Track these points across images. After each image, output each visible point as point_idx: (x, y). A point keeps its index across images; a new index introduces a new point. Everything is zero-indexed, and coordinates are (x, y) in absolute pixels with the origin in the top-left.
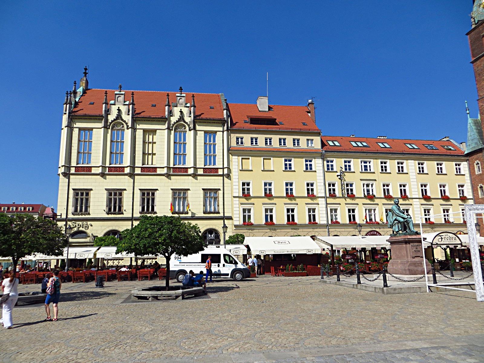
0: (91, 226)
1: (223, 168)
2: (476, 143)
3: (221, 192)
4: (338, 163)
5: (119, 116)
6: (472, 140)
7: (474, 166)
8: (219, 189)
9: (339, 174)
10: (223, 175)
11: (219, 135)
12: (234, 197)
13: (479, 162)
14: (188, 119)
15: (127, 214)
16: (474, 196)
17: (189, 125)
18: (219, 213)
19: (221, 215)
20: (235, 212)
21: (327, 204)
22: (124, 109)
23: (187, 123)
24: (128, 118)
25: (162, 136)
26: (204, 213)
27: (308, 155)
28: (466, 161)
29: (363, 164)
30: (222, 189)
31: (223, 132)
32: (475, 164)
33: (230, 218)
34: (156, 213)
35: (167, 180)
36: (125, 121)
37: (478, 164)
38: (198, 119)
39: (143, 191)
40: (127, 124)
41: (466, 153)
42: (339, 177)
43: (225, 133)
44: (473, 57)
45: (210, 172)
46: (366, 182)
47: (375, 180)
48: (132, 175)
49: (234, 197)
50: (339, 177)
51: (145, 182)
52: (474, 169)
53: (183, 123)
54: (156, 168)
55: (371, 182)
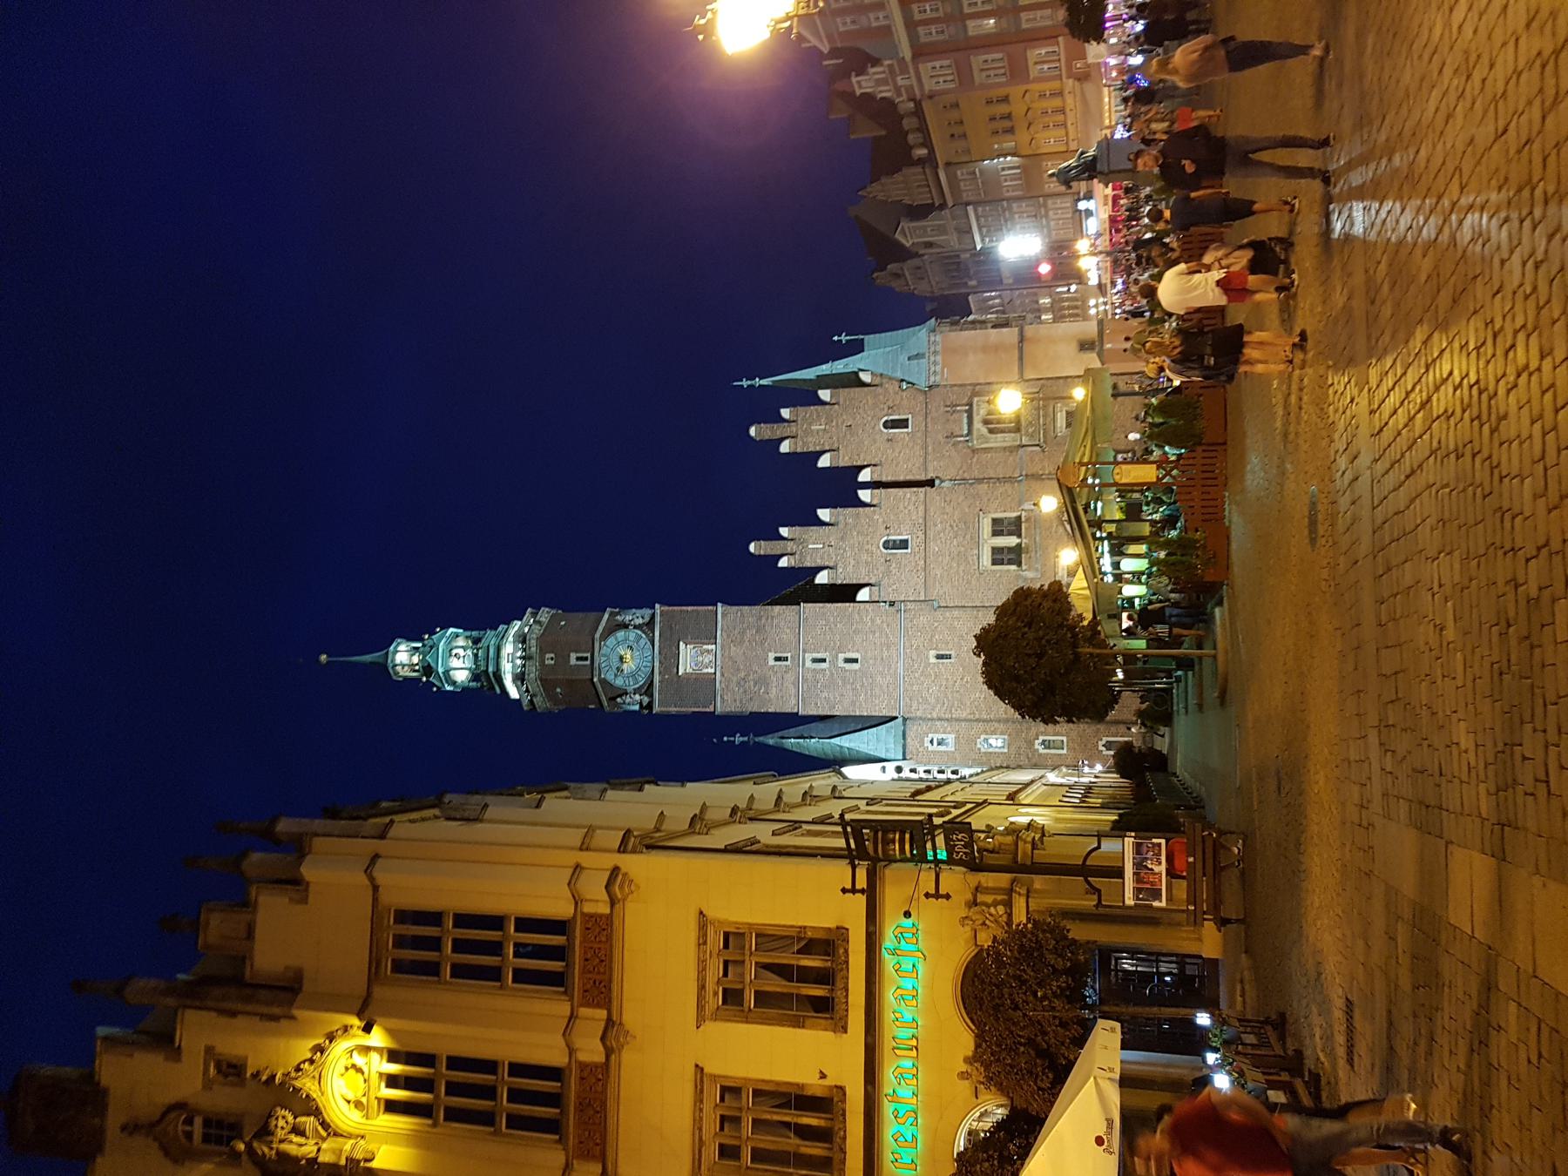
32: (931, 748)
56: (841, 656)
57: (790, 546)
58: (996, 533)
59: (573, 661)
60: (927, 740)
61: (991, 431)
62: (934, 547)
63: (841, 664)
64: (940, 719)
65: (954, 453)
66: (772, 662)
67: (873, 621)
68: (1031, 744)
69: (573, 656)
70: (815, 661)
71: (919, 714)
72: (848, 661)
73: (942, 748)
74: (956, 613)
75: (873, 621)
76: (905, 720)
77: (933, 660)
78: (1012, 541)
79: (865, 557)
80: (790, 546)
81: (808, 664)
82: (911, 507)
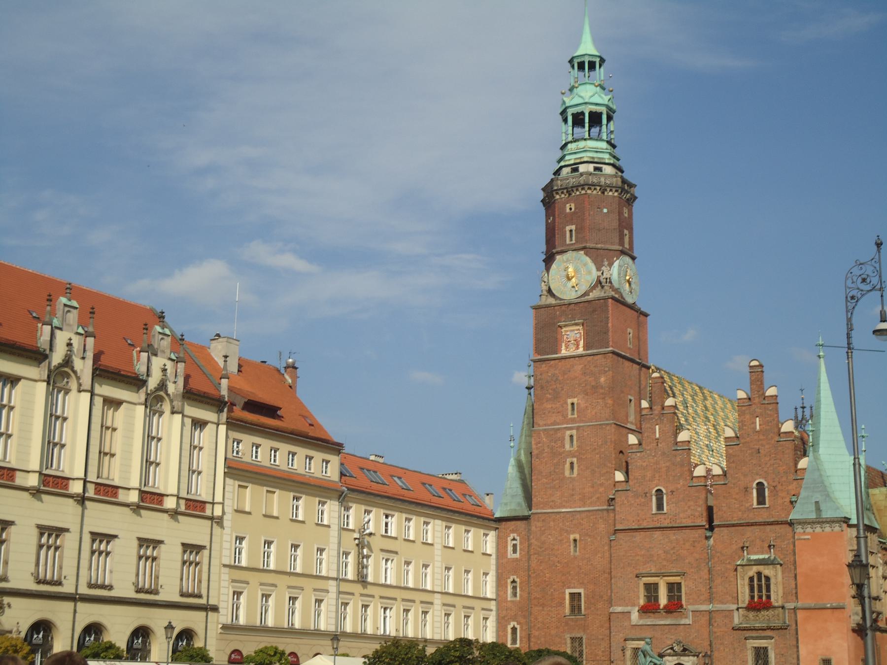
0: (9, 606)
1: (213, 503)
2: (519, 504)
3: (206, 552)
4: (355, 514)
5: (67, 362)
6: (513, 496)
7: (506, 542)
8: (204, 547)
9: (357, 535)
10: (211, 518)
11: (210, 428)
12: (225, 566)
13: (518, 538)
14: (171, 388)
15: (68, 588)
16: (498, 595)
17: (171, 401)
18: (199, 596)
19: (203, 601)
20: (223, 598)
21: (340, 593)
22: (76, 341)
23: (168, 395)
24: (84, 367)
25: (132, 417)
26: (182, 595)
27: (319, 489)
28: (496, 529)
29: (384, 520)
30: (208, 547)
31: (218, 425)
32: (509, 539)
33: (215, 609)
34: (110, 588)
35: (134, 516)
36: (75, 372)
37: (514, 539)
38: (191, 395)
39: (96, 536)
40: (78, 378)
41: (496, 516)
42: (357, 542)
43: (223, 428)
44: (538, 351)
45: (195, 507)
46: (386, 555)
47: (396, 553)
48: (82, 500)
49: (225, 566)
50: (357, 542)
51: (101, 517)
52: (506, 547)
53: (162, 393)
54: (117, 487)
55: (391, 556)
56: (575, 460)
57: (657, 408)
58: (671, 587)
59: (568, 228)
60: (515, 535)
61: (751, 579)
62: (657, 534)
63: (569, 460)
64: (529, 545)
65: (734, 547)
66: (570, 401)
67: (601, 485)
68: (514, 619)
69: (573, 227)
70: (571, 436)
71: (533, 528)
72: (572, 463)
73: (510, 548)
74: (607, 555)
75: (601, 485)
76: (526, 518)
77: (572, 537)
78: (663, 601)
79: (649, 474)
80: (657, 408)
81: (568, 433)
82: (689, 512)
